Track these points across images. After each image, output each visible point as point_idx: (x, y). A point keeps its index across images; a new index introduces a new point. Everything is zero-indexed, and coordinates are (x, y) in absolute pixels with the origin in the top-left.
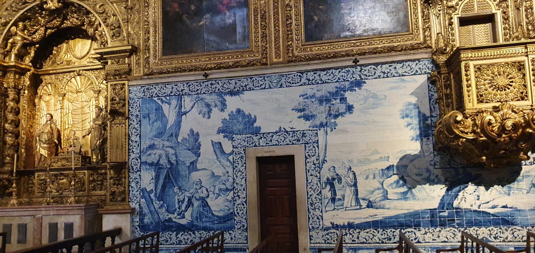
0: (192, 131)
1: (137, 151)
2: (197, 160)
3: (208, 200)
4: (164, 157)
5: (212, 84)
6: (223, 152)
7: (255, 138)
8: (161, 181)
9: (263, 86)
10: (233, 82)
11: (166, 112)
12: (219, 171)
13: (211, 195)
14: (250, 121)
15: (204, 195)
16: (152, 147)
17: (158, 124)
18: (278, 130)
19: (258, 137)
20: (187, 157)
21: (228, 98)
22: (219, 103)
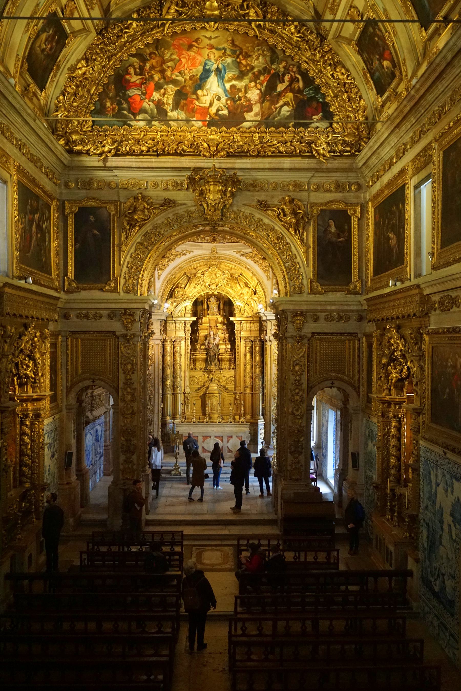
17: (429, 486)
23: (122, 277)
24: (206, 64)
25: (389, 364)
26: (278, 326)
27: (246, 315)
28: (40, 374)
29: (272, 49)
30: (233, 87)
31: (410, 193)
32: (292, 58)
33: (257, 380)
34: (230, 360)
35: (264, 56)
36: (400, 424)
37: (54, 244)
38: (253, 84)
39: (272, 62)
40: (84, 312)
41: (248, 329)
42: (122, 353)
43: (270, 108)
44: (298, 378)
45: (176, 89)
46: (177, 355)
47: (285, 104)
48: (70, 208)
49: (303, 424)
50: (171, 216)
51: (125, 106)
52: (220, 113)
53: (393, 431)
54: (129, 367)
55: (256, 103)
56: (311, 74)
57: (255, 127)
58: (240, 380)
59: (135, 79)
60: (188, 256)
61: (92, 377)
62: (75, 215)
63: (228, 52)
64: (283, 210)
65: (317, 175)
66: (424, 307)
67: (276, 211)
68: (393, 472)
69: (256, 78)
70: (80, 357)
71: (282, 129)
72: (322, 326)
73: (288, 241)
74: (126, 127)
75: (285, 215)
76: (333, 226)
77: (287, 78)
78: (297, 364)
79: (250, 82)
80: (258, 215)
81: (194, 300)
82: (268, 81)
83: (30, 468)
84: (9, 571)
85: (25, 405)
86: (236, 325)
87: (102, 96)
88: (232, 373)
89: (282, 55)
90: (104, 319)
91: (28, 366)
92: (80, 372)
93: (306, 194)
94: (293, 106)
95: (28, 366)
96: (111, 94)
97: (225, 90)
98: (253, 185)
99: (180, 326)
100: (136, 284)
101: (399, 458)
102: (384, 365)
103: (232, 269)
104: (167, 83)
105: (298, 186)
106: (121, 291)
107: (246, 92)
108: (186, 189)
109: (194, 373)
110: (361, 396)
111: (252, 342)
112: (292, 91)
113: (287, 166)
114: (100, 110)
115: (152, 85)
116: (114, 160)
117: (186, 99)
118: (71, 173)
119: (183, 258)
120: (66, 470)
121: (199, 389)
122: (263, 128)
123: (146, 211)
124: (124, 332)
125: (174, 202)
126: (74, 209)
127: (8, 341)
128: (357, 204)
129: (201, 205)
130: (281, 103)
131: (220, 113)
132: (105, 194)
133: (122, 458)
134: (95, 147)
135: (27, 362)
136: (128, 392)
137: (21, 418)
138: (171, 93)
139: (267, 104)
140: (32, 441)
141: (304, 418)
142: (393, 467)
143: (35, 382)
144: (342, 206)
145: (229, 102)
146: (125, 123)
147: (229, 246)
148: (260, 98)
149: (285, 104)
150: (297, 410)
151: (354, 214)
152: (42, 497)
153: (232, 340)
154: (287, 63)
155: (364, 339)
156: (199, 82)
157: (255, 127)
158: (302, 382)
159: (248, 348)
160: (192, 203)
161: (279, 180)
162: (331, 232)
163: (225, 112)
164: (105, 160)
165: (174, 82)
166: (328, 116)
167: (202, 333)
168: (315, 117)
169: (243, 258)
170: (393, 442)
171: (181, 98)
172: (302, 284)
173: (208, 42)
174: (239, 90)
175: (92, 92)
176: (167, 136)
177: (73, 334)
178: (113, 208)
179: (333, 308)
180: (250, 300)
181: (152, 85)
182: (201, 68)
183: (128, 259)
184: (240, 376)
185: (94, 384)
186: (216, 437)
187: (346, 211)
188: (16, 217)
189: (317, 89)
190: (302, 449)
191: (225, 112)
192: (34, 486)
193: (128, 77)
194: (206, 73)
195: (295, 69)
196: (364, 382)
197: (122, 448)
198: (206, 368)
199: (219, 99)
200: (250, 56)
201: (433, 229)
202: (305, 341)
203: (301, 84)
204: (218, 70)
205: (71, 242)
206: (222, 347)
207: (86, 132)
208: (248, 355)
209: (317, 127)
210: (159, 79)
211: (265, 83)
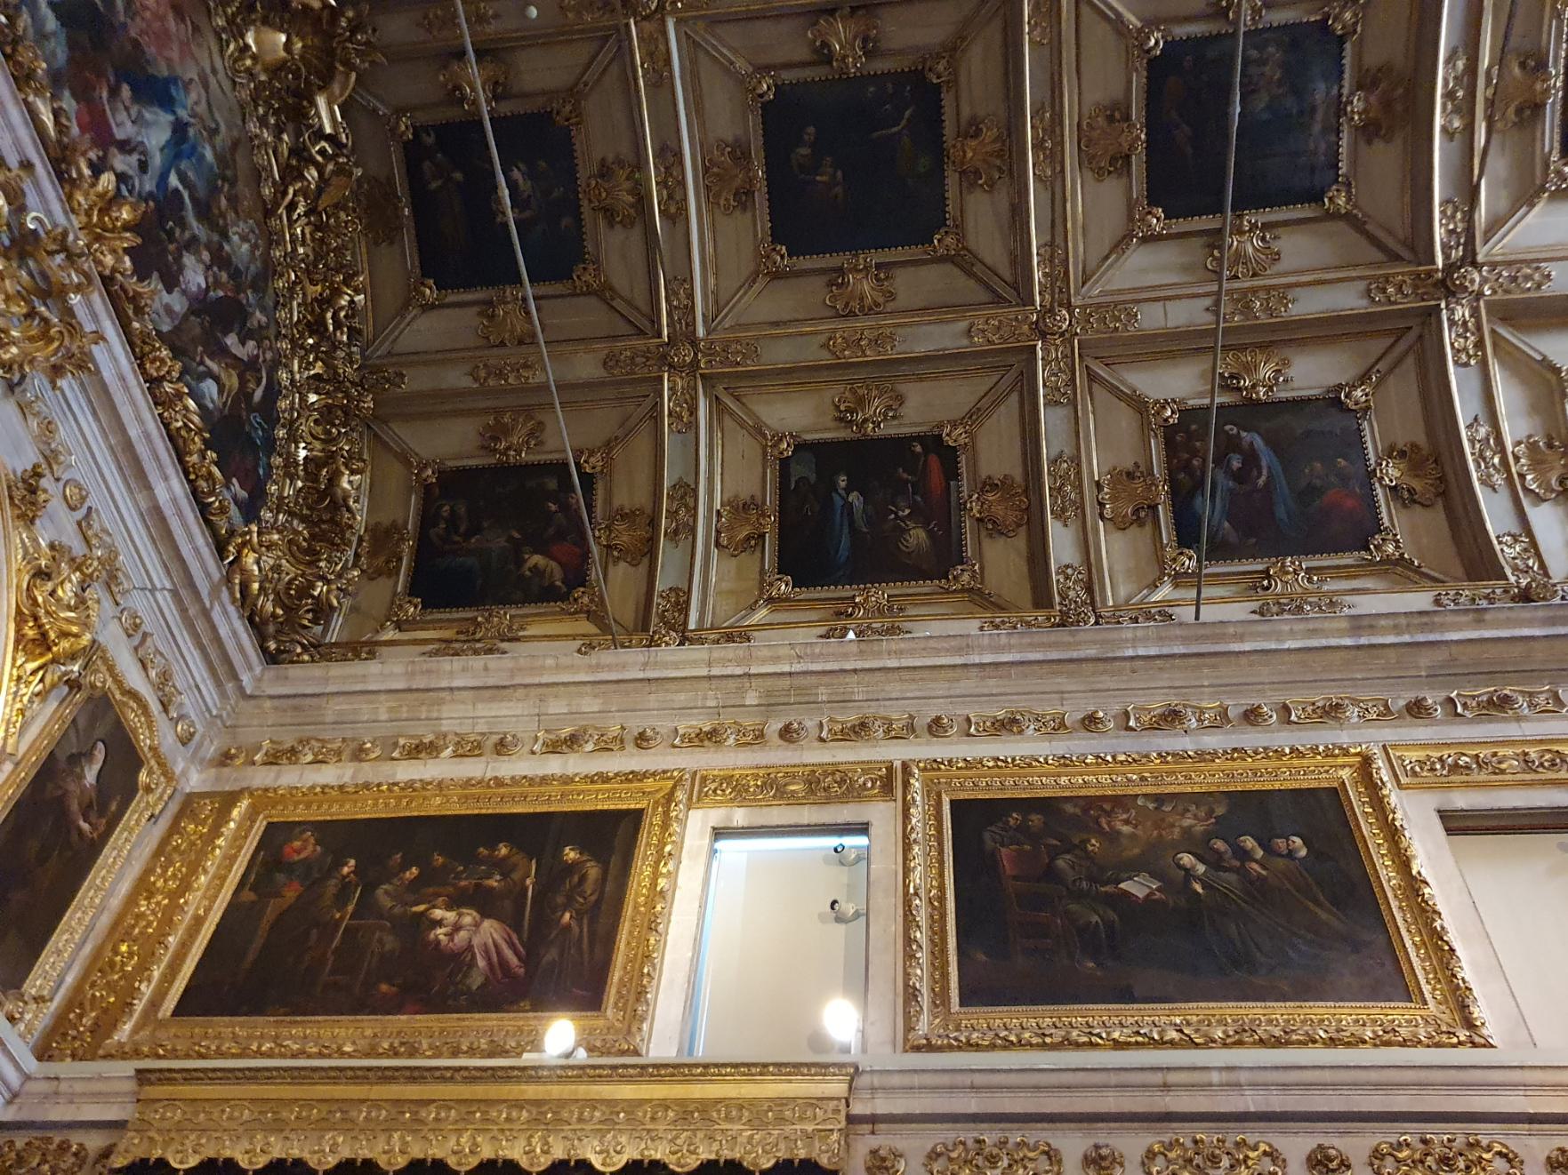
29: (269, 270)
32: (278, 335)
35: (252, 252)
38: (206, 256)
39: (254, 287)
63: (218, 140)
65: (164, 599)
69: (220, 260)
76: (97, 767)
79: (208, 247)
94: (225, 404)
97: (163, 177)
144: (144, 741)
149: (217, 379)
154: (267, 327)
162: (81, 777)
173: (208, 71)
174: (182, 224)
182: (164, 72)
195: (269, 355)
200: (237, 213)
204: (179, 129)
211: (221, 294)
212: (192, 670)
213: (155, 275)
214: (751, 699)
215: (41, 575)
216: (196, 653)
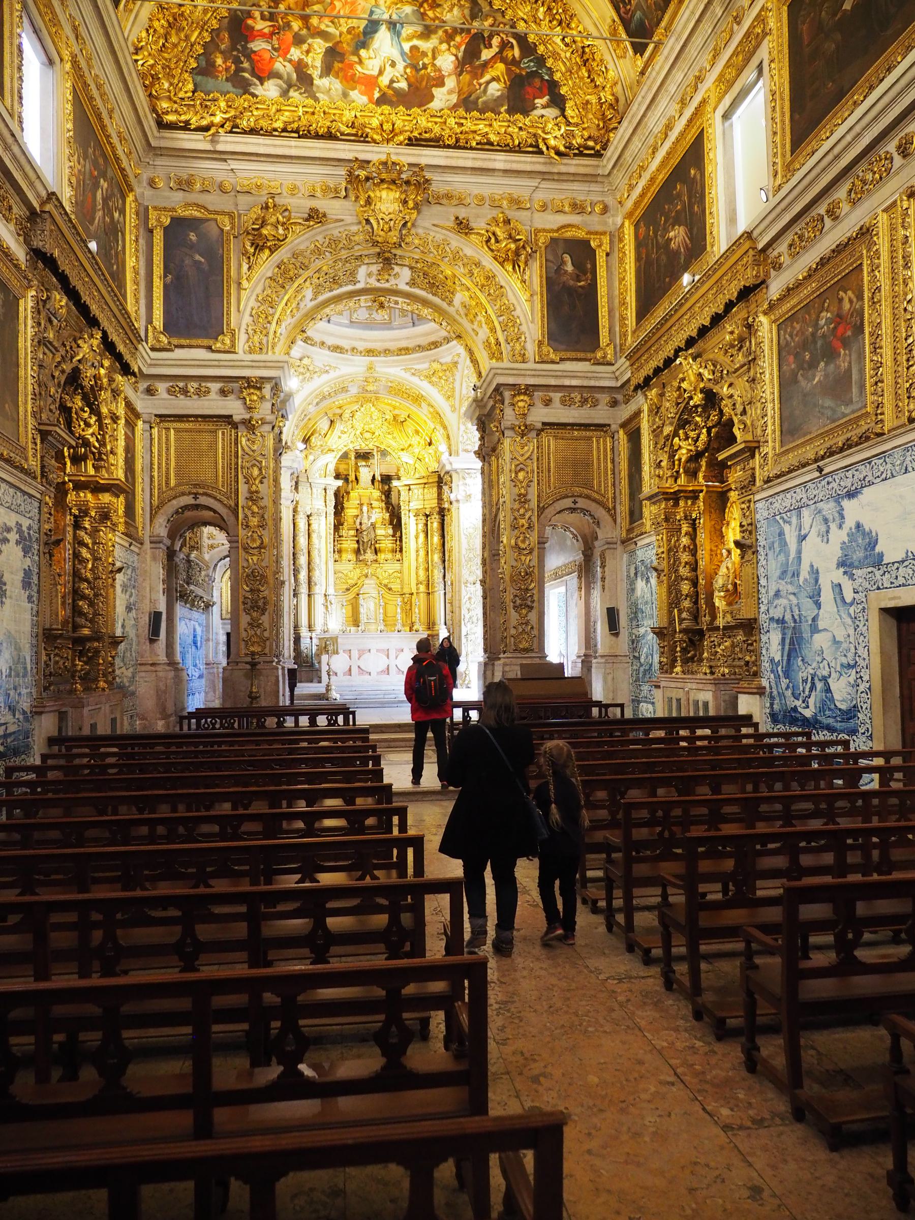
0: (812, 566)
1: (766, 602)
2: (818, 615)
3: (830, 681)
4: (788, 611)
5: (828, 483)
6: (843, 599)
7: (878, 573)
8: (787, 647)
9: (884, 476)
10: (849, 474)
11: (788, 540)
12: (840, 635)
13: (833, 675)
14: (873, 543)
15: (825, 673)
16: (777, 594)
17: (782, 558)
18: (904, 556)
19: (881, 572)
20: (808, 610)
21: (845, 503)
22: (837, 515)
23: (243, 330)
24: (372, 12)
25: (676, 434)
26: (482, 438)
27: (417, 476)
28: (109, 448)
30: (414, 48)
31: (715, 128)
32: (503, 14)
33: (436, 571)
34: (394, 551)
35: (461, 6)
36: (695, 529)
37: (130, 262)
38: (444, 46)
39: (473, 17)
40: (181, 385)
41: (421, 497)
42: (243, 450)
43: (470, 84)
44: (523, 491)
45: (328, 45)
46: (314, 536)
47: (493, 79)
48: (158, 220)
49: (535, 562)
50: (320, 238)
51: (246, 65)
52: (395, 85)
53: (685, 541)
54: (256, 472)
55: (449, 75)
56: (531, 38)
57: (450, 109)
58: (410, 574)
59: (261, 25)
60: (333, 374)
61: (194, 491)
62: (166, 230)
64: (494, 234)
65: (544, 185)
66: (758, 272)
67: (483, 235)
68: (686, 604)
69: (449, 37)
70: (173, 459)
71: (489, 114)
72: (559, 413)
73: (503, 283)
74: (247, 96)
75: (497, 241)
77: (496, 41)
78: (522, 469)
79: (441, 43)
80: (456, 241)
81: (340, 453)
82: (467, 44)
83: (91, 604)
84: (56, 734)
85: (82, 495)
86: (402, 493)
87: (210, 48)
88: (397, 566)
89: (488, 8)
90: (213, 395)
91: (88, 425)
92: (173, 483)
93: (528, 213)
95: (88, 425)
96: (223, 47)
97: (403, 53)
98: (449, 196)
99: (318, 492)
100: (264, 342)
101: (695, 583)
102: (667, 438)
103: (395, 408)
104: (313, 36)
105: (516, 202)
106: (241, 352)
107: (434, 58)
108: (345, 197)
109: (339, 566)
110: (619, 520)
111: (427, 516)
112: (504, 60)
113: (499, 166)
114: (206, 70)
115: (289, 36)
116: (229, 139)
117: (342, 62)
118: (159, 162)
119: (325, 377)
120: (152, 641)
121: (348, 590)
122: (461, 112)
123: (280, 228)
124: (247, 416)
125: (324, 215)
126: (163, 219)
127: (55, 321)
128: (604, 233)
129: (368, 221)
130: (487, 77)
131: (395, 85)
132: (214, 201)
133: (245, 619)
134: (199, 116)
135: (86, 415)
136: (253, 513)
137: (75, 516)
138: (319, 51)
139: (466, 77)
140: (96, 559)
141: (535, 553)
142: (687, 596)
143: (101, 459)
144: (581, 235)
145: (408, 70)
146: (246, 92)
147: (394, 361)
148: (456, 68)
149: (493, 79)
150: (523, 541)
151: (600, 246)
152: (113, 657)
153: (396, 521)
154: (495, 20)
155: (621, 432)
156: (362, 38)
157: (450, 109)
158: (528, 497)
159: (421, 526)
160: (354, 219)
161: (486, 192)
163: (403, 85)
164: (214, 140)
165: (324, 35)
166: (558, 102)
167: (350, 511)
168: (539, 102)
169: (415, 380)
170: (685, 557)
171: (334, 58)
172: (524, 348)
174: (424, 54)
175: (193, 39)
176: (313, 113)
177: (161, 421)
178: (227, 220)
179: (574, 382)
180: (423, 453)
181: (289, 36)
183: (252, 303)
184: (409, 569)
185: (198, 502)
186: (378, 651)
187: (588, 242)
188: (69, 131)
189: (541, 61)
190: (533, 602)
191: (403, 85)
192: (97, 636)
193: (250, 22)
194: (373, 26)
196: (624, 497)
197: (244, 603)
198: (358, 560)
199: (393, 64)
201: (775, 133)
202: (534, 434)
203: (517, 52)
204: (392, 25)
205: (158, 270)
206: (380, 532)
207: (182, 99)
208: (422, 536)
209: (542, 116)
210: (300, 29)
211: (463, 47)
212: (579, 191)
213: (435, 91)
214: (719, 11)
215: (488, 241)
216: (576, 184)
